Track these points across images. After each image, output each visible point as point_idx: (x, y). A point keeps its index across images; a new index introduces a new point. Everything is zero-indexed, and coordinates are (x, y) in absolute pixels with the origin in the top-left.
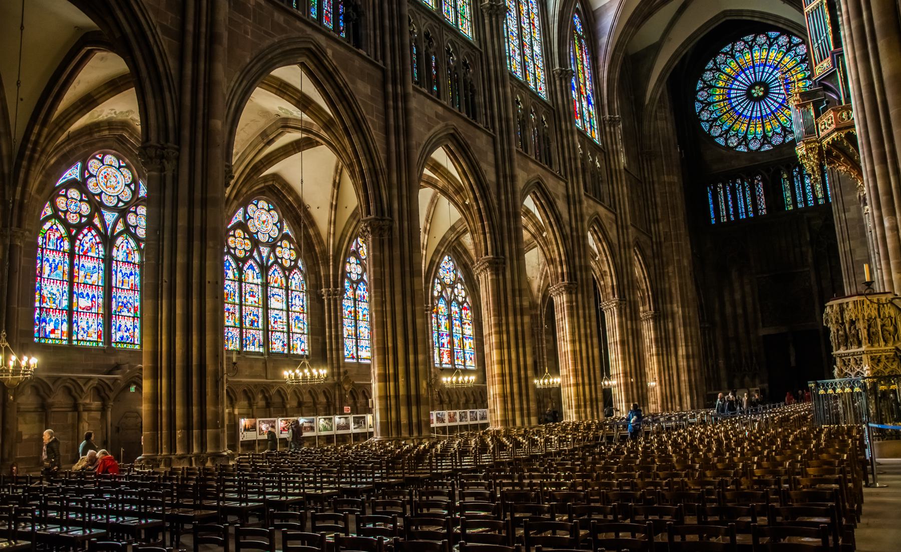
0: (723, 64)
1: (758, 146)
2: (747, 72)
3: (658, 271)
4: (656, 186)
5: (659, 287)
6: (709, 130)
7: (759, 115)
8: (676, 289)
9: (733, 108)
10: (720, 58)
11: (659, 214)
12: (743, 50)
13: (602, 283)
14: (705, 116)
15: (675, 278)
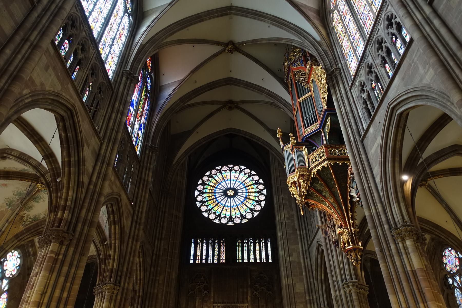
0: (215, 174)
1: (226, 222)
2: (227, 182)
3: (151, 277)
4: (166, 215)
5: (149, 291)
6: (200, 207)
7: (229, 205)
8: (162, 295)
9: (216, 198)
10: (214, 172)
11: (164, 235)
12: (226, 170)
13: (103, 267)
14: (199, 198)
15: (164, 287)
